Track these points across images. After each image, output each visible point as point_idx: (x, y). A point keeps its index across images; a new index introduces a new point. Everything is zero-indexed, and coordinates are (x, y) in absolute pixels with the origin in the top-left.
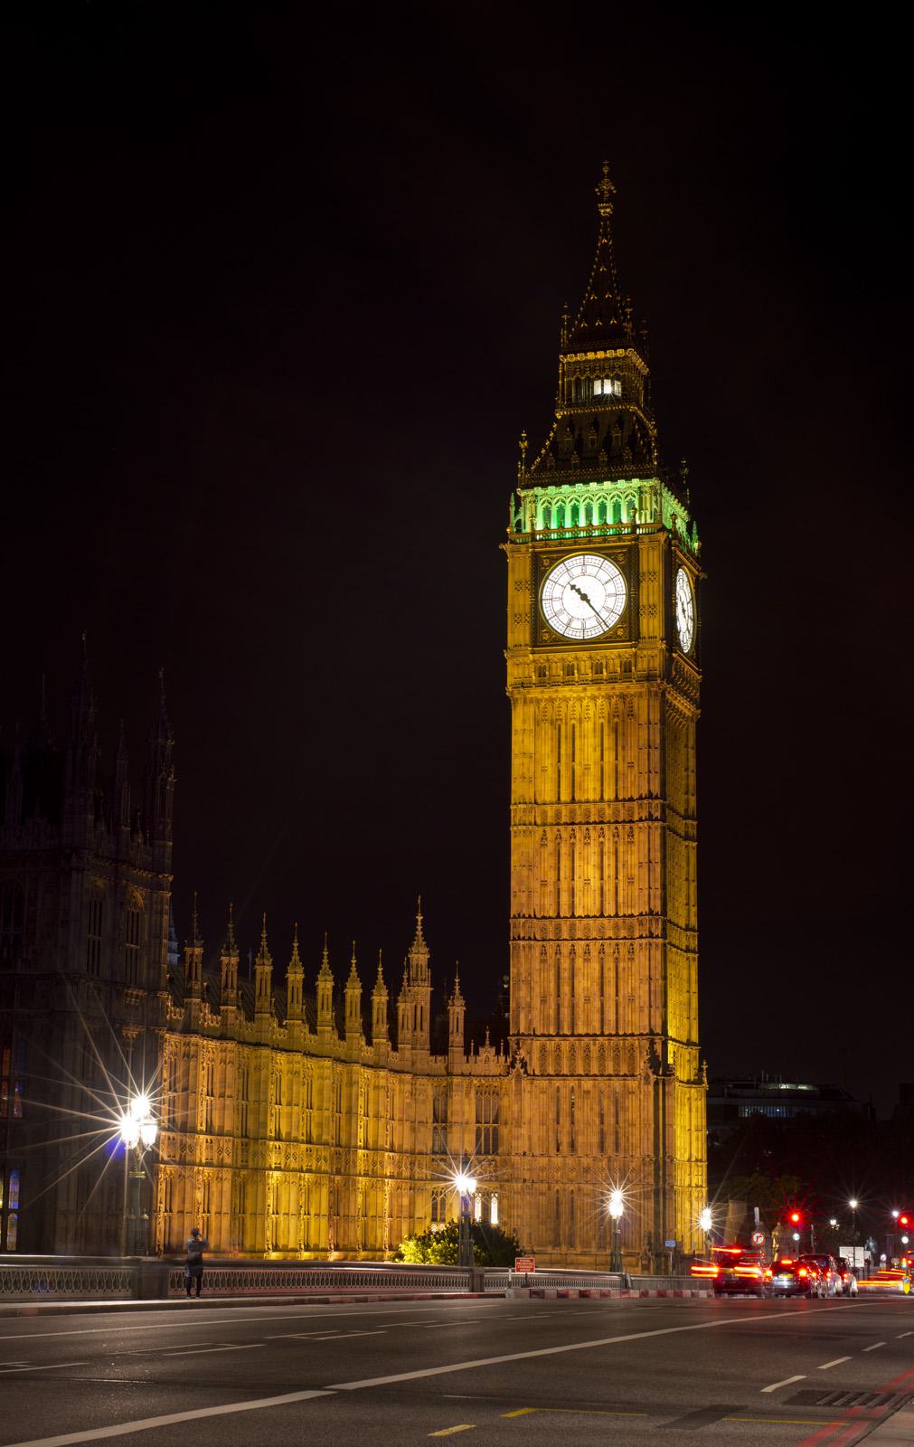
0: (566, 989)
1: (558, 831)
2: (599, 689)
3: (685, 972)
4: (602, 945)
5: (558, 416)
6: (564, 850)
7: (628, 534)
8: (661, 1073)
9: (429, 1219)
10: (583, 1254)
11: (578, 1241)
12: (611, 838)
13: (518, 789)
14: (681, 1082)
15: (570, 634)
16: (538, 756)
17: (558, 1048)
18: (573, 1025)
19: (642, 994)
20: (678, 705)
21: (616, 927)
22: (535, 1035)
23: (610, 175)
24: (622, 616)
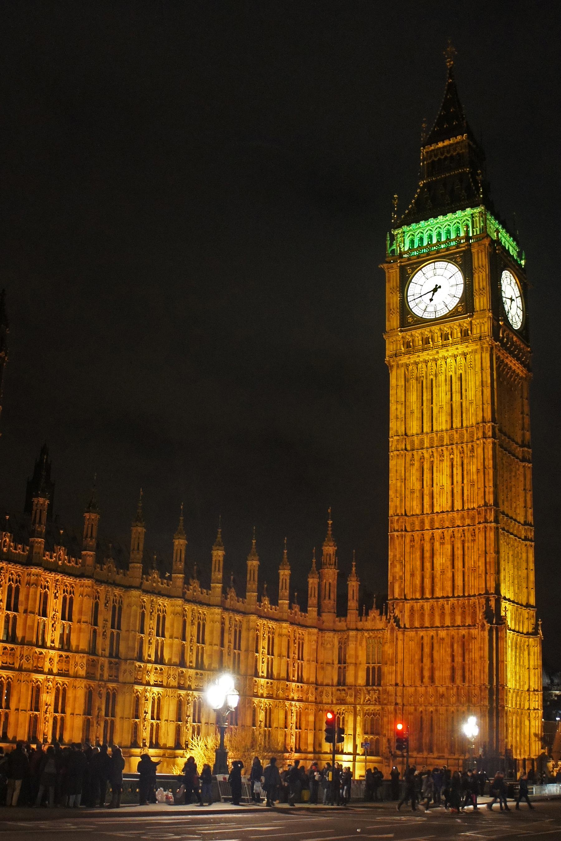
0: (428, 565)
1: (422, 453)
2: (448, 351)
3: (524, 555)
4: (453, 532)
6: (426, 466)
7: (463, 243)
8: (494, 622)
10: (439, 758)
11: (435, 748)
12: (459, 454)
13: (395, 426)
15: (426, 316)
16: (407, 403)
17: (422, 607)
20: (510, 364)
21: (463, 518)
22: (406, 599)
24: (460, 299)
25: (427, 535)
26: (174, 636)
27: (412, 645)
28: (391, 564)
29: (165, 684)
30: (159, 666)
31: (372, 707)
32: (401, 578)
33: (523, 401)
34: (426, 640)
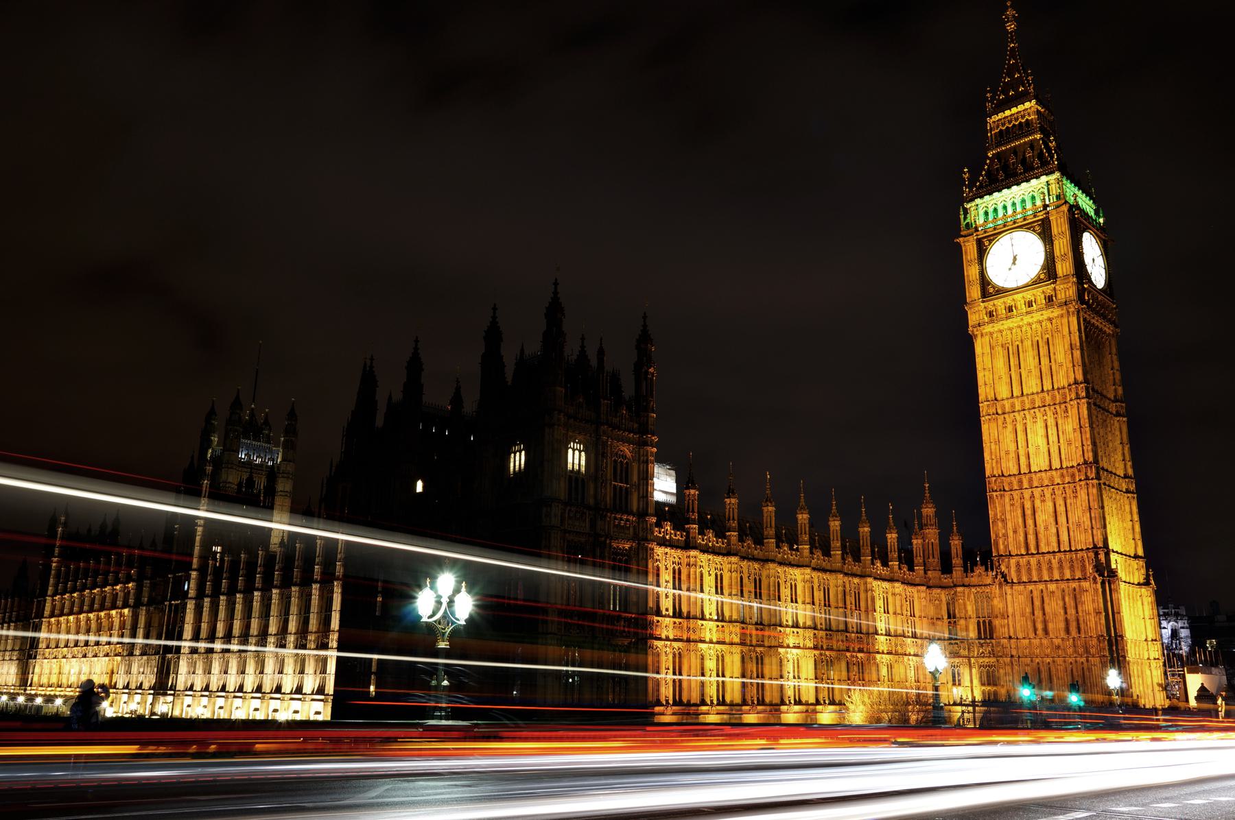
0: (1030, 522)
1: (1014, 416)
4: (1053, 489)
5: (990, 155)
6: (1020, 428)
8: (1106, 575)
9: (950, 683)
12: (1052, 415)
14: (1125, 582)
17: (1029, 563)
18: (1037, 547)
19: (1085, 520)
21: (1062, 476)
23: (1011, 6)
24: (1042, 266)
25: (1027, 494)
26: (806, 601)
27: (1022, 598)
28: (992, 522)
29: (802, 646)
30: (795, 630)
31: (987, 660)
32: (1004, 535)
33: (1112, 357)
34: (1036, 594)
